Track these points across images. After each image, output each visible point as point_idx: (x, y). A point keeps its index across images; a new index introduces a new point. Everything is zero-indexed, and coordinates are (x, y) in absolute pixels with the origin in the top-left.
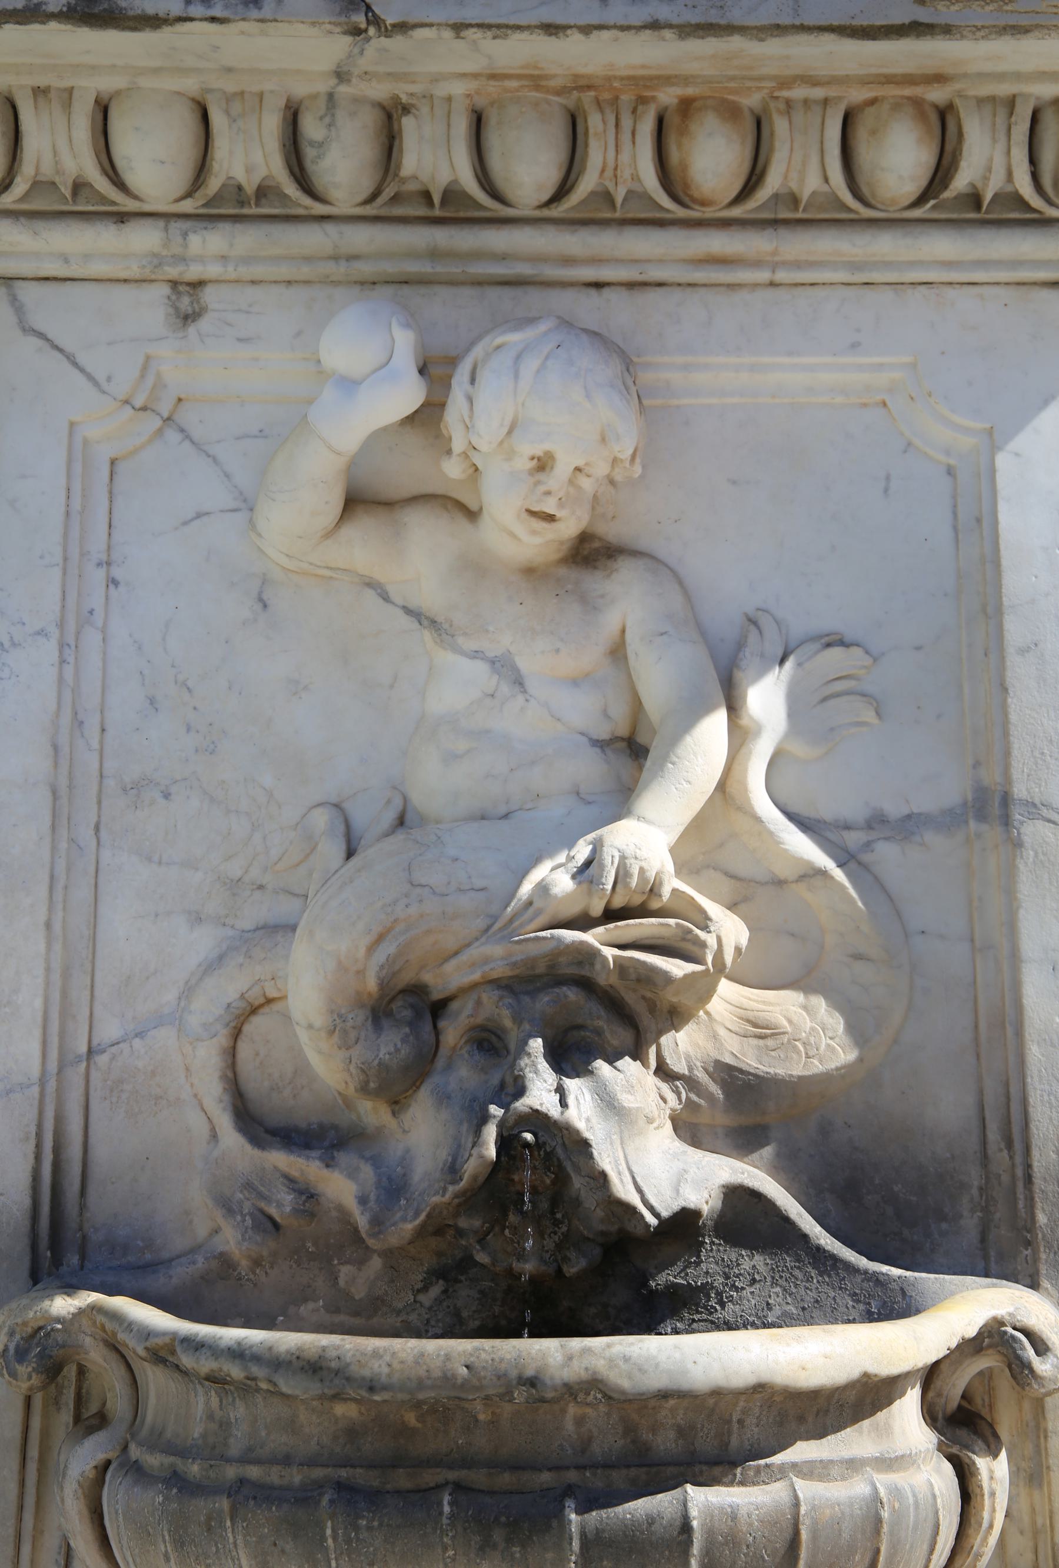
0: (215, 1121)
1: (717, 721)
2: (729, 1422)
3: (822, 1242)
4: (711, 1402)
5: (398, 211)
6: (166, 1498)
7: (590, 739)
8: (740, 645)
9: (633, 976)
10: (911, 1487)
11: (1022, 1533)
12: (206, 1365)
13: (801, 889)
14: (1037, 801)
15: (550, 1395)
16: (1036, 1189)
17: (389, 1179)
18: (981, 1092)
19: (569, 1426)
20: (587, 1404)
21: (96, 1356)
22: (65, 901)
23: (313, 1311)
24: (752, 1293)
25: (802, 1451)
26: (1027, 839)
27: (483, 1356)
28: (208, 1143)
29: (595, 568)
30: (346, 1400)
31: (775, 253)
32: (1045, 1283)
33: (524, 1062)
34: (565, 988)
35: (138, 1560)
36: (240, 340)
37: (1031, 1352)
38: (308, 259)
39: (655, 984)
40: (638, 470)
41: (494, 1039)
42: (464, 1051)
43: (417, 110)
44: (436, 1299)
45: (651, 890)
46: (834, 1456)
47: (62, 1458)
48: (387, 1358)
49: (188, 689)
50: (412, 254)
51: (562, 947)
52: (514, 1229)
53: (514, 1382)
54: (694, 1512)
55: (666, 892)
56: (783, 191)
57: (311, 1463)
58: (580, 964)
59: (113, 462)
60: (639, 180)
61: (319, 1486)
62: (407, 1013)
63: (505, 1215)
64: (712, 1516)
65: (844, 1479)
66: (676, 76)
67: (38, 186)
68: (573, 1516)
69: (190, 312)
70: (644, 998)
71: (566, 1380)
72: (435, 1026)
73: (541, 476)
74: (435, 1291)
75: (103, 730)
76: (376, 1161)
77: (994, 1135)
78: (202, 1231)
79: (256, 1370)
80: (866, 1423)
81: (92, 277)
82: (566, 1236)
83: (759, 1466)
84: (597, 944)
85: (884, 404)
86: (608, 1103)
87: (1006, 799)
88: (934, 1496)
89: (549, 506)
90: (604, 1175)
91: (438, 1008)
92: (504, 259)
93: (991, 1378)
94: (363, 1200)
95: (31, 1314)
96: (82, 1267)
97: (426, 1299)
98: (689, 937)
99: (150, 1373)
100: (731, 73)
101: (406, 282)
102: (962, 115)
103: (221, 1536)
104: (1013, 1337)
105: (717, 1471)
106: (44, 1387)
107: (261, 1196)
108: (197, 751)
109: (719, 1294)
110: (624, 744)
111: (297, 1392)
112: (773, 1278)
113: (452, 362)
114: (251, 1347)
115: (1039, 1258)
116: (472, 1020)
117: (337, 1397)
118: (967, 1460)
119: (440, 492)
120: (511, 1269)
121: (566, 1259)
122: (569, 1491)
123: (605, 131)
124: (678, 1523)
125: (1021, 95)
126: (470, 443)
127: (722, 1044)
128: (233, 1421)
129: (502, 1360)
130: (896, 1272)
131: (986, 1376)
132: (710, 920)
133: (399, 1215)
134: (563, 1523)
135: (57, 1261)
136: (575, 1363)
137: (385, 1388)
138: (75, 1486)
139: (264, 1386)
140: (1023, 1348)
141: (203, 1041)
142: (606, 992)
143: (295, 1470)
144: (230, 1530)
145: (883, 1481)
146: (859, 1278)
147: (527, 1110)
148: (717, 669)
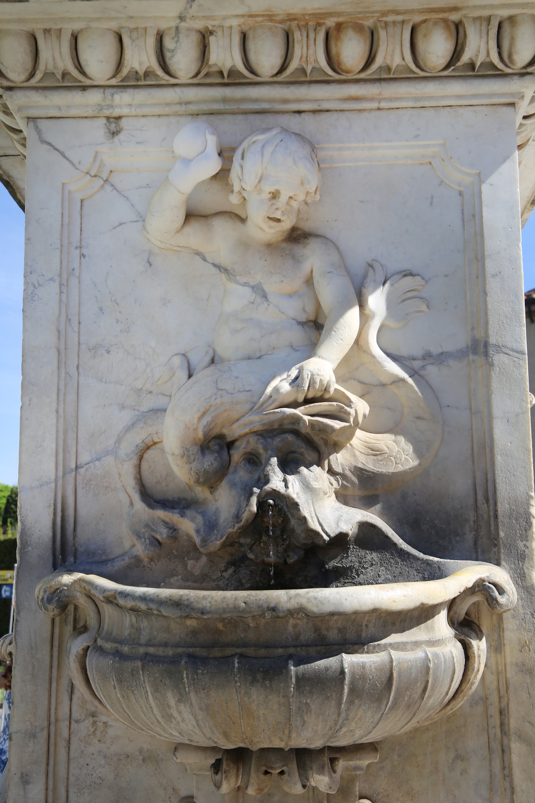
0: (132, 497)
1: (354, 313)
2: (361, 626)
3: (403, 547)
4: (353, 617)
5: (208, 81)
6: (113, 662)
7: (297, 322)
8: (365, 277)
9: (317, 429)
10: (443, 653)
11: (492, 673)
12: (130, 604)
13: (393, 388)
14: (500, 345)
15: (281, 615)
16: (499, 521)
17: (209, 522)
18: (474, 478)
19: (290, 628)
20: (298, 619)
21: (82, 601)
22: (64, 400)
23: (177, 581)
24: (371, 570)
25: (394, 638)
26: (496, 363)
27: (252, 598)
28: (129, 507)
29: (299, 243)
30: (191, 618)
31: (380, 94)
32: (503, 563)
33: (269, 468)
34: (287, 435)
35: (102, 689)
36: (138, 143)
37: (496, 593)
38: (168, 104)
39: (327, 432)
40: (318, 197)
41: (255, 458)
42: (242, 464)
43: (216, 33)
44: (231, 575)
45: (325, 389)
46: (408, 640)
47: (68, 645)
48: (209, 599)
49: (117, 303)
50: (215, 101)
51: (285, 416)
52: (265, 544)
53: (266, 609)
54: (346, 665)
55: (332, 390)
56: (384, 65)
57: (177, 645)
58: (293, 423)
59: (82, 201)
60: (318, 62)
61: (180, 656)
62: (216, 447)
63: (261, 537)
64: (354, 667)
65: (412, 650)
66: (334, 13)
68: (292, 668)
69: (115, 131)
70: (322, 438)
71: (289, 608)
72: (229, 453)
73: (274, 201)
74: (230, 571)
75: (80, 323)
76: (203, 514)
77: (480, 497)
78: (127, 545)
79: (152, 606)
80: (423, 625)
81: (72, 116)
82: (288, 546)
83: (375, 645)
84: (301, 415)
85: (430, 163)
86: (307, 486)
87: (486, 344)
88: (453, 657)
89: (278, 215)
90: (305, 518)
91: (230, 445)
92: (256, 101)
93: (478, 605)
94: (198, 531)
95: (53, 583)
96: (75, 562)
97: (226, 575)
98: (342, 410)
99: (105, 607)
100: (359, 10)
101: (212, 114)
102: (466, 26)
103: (138, 678)
104: (488, 587)
105: (356, 647)
106: (60, 615)
107: (153, 530)
108: (121, 331)
109: (357, 571)
110: (312, 324)
111: (170, 615)
112: (381, 563)
113: (233, 150)
114: (149, 595)
115: (501, 552)
116: (245, 450)
117: (187, 617)
118: (468, 642)
119: (228, 210)
120: (264, 561)
121: (288, 556)
122: (290, 657)
123: (302, 39)
124: (339, 670)
125: (493, 15)
126: (242, 187)
127: (358, 459)
128: (142, 628)
129: (260, 600)
130: (436, 559)
131: (476, 605)
132: (352, 402)
133: (214, 537)
134: (288, 671)
135: (64, 560)
136: (293, 600)
137: (208, 613)
138: (74, 657)
139: (155, 612)
140: (493, 592)
141: (126, 461)
142: (305, 436)
143: (170, 649)
144: (142, 675)
145: (430, 651)
146: (419, 562)
147: (271, 490)
148: (354, 287)
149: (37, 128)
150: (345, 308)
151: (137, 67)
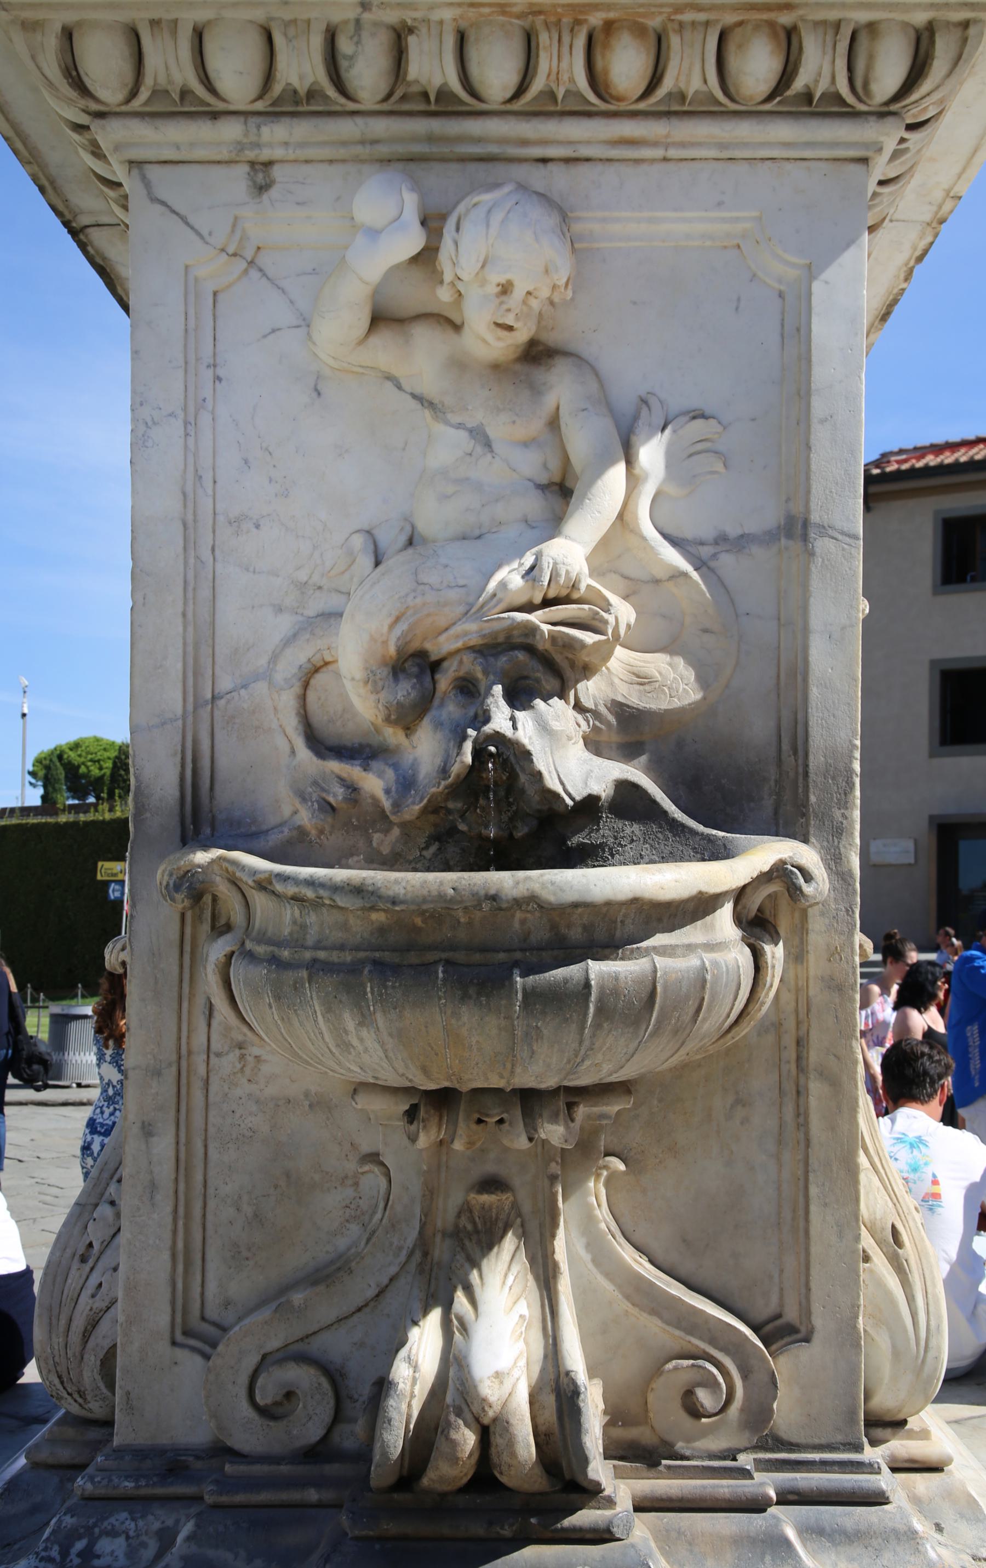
0: (293, 742)
1: (618, 472)
2: (615, 922)
3: (676, 816)
4: (605, 909)
5: (406, 107)
6: (268, 971)
7: (535, 484)
8: (636, 418)
9: (560, 643)
10: (725, 961)
11: (789, 991)
12: (291, 890)
13: (670, 586)
14: (826, 525)
15: (504, 905)
16: (810, 780)
17: (404, 777)
18: (779, 719)
19: (516, 925)
20: (528, 911)
21: (223, 888)
22: (194, 598)
23: (357, 862)
24: (631, 848)
25: (660, 939)
26: (818, 551)
27: (464, 882)
28: (290, 756)
29: (540, 364)
30: (378, 910)
31: (667, 136)
32: (813, 840)
33: (490, 700)
34: (516, 652)
35: (253, 1008)
36: (298, 204)
37: (801, 880)
38: (344, 144)
39: (575, 649)
40: (569, 294)
41: (470, 686)
42: (451, 694)
43: (419, 30)
44: (433, 854)
45: (573, 586)
46: (678, 942)
47: (205, 951)
48: (404, 884)
49: (270, 453)
50: (415, 139)
51: (515, 624)
52: (483, 809)
53: (483, 898)
54: (592, 976)
55: (583, 587)
56: (675, 90)
57: (357, 948)
58: (526, 635)
59: (215, 294)
60: (574, 82)
61: (362, 962)
62: (415, 670)
63: (477, 800)
64: (603, 978)
65: (684, 956)
66: (602, 4)
67: (157, 93)
68: (518, 979)
69: (264, 184)
70: (567, 658)
71: (515, 896)
72: (433, 678)
73: (504, 298)
74: (433, 849)
75: (215, 482)
76: (395, 766)
77: (786, 746)
78: (287, 811)
79: (322, 892)
80: (699, 923)
81: (197, 160)
82: (516, 813)
83: (633, 948)
84: (537, 622)
85: (739, 246)
86: (543, 727)
87: (806, 523)
88: (738, 967)
90: (540, 774)
91: (435, 666)
92: (479, 141)
93: (776, 898)
94: (387, 792)
95: (182, 863)
96: (213, 835)
97: (428, 854)
98: (597, 617)
99: (256, 897)
101: (412, 160)
102: (803, 34)
103: (303, 993)
104: (791, 871)
105: (607, 951)
106: (192, 907)
107: (323, 790)
108: (276, 495)
109: (611, 849)
110: (556, 488)
111: (348, 905)
112: (644, 838)
113: (443, 217)
114: (319, 878)
115: (810, 824)
116: (456, 673)
117: (373, 908)
118: (759, 947)
119: (436, 311)
120: (481, 834)
121: (515, 827)
122: (516, 964)
123: (551, 45)
124: (582, 982)
125: (845, 19)
126: (456, 275)
127: (616, 689)
128: (308, 924)
129: (475, 885)
130: (721, 834)
131: (773, 897)
132: (611, 605)
133: (410, 800)
134: (512, 983)
135: (197, 831)
136: (521, 886)
137: (402, 902)
138: (213, 966)
139: (327, 902)
140: (797, 878)
141: (285, 690)
142: (543, 654)
143: (347, 953)
144: (308, 989)
145: (708, 957)
146: (698, 838)
147: (492, 732)
148: (619, 435)
149: (144, 178)
150: (604, 464)
151: (296, 83)
